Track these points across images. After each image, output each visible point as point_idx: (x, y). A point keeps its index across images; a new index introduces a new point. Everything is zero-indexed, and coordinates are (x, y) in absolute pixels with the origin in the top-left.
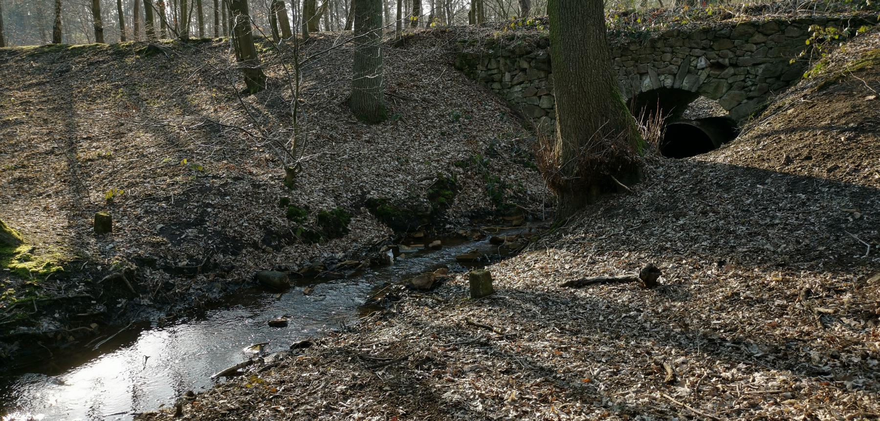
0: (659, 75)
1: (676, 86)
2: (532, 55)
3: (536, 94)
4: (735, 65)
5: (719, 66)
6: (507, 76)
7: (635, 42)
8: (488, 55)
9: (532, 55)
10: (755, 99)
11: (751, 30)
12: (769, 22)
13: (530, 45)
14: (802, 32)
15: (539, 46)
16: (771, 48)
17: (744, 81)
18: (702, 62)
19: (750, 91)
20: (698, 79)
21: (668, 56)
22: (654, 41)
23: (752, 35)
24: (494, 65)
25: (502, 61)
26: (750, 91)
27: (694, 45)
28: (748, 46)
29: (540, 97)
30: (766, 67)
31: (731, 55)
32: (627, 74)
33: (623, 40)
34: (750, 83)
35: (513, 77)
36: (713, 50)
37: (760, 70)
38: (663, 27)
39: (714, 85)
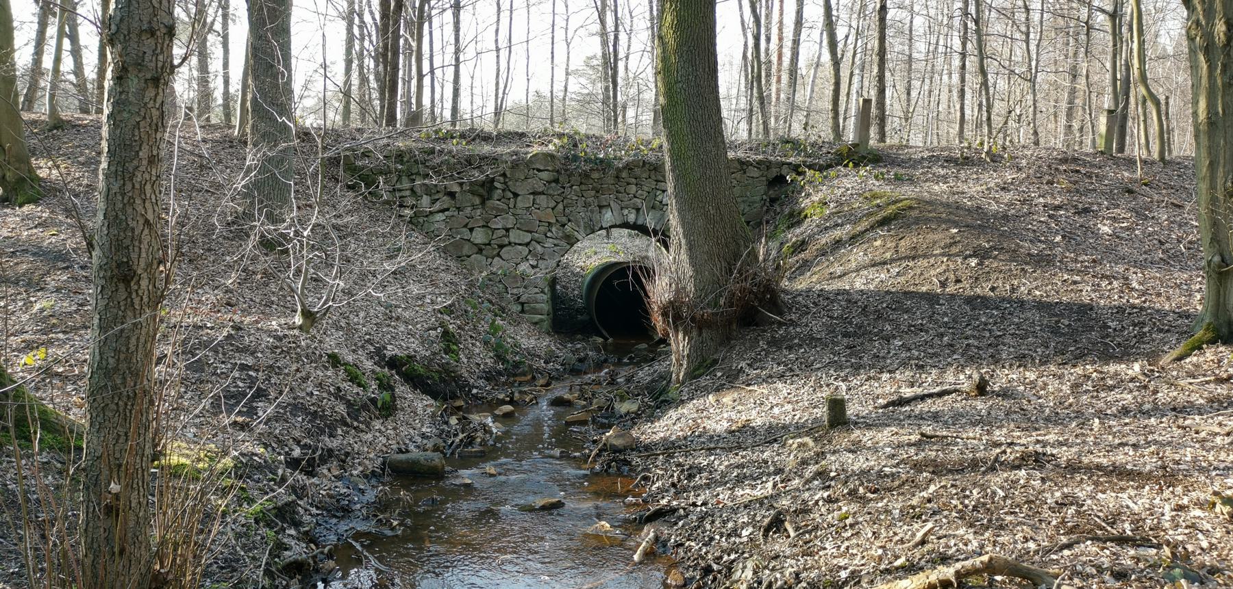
3: (466, 226)
21: (633, 189)
22: (619, 170)
29: (471, 230)
32: (586, 205)
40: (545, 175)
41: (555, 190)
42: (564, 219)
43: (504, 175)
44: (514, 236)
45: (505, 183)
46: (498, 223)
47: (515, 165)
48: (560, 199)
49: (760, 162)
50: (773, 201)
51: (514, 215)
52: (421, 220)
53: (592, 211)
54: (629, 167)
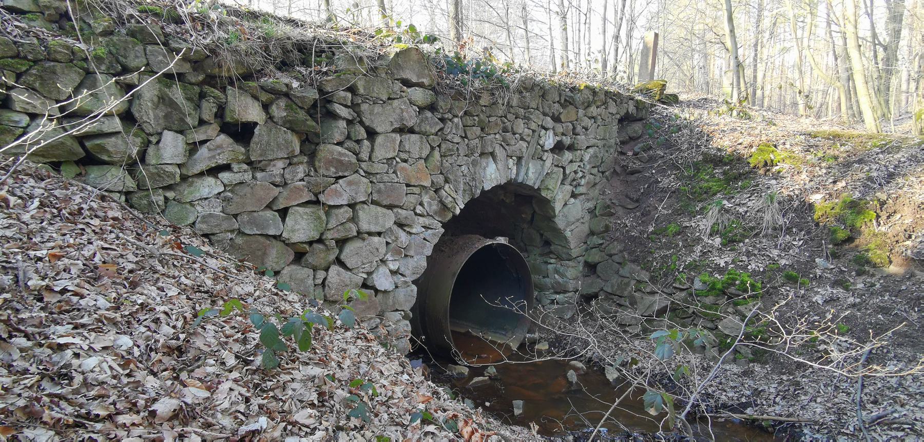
18: (549, 141)
20: (543, 166)
29: (283, 213)
35: (193, 148)
41: (431, 123)
43: (352, 90)
44: (369, 218)
45: (354, 106)
46: (340, 194)
48: (436, 140)
51: (368, 174)
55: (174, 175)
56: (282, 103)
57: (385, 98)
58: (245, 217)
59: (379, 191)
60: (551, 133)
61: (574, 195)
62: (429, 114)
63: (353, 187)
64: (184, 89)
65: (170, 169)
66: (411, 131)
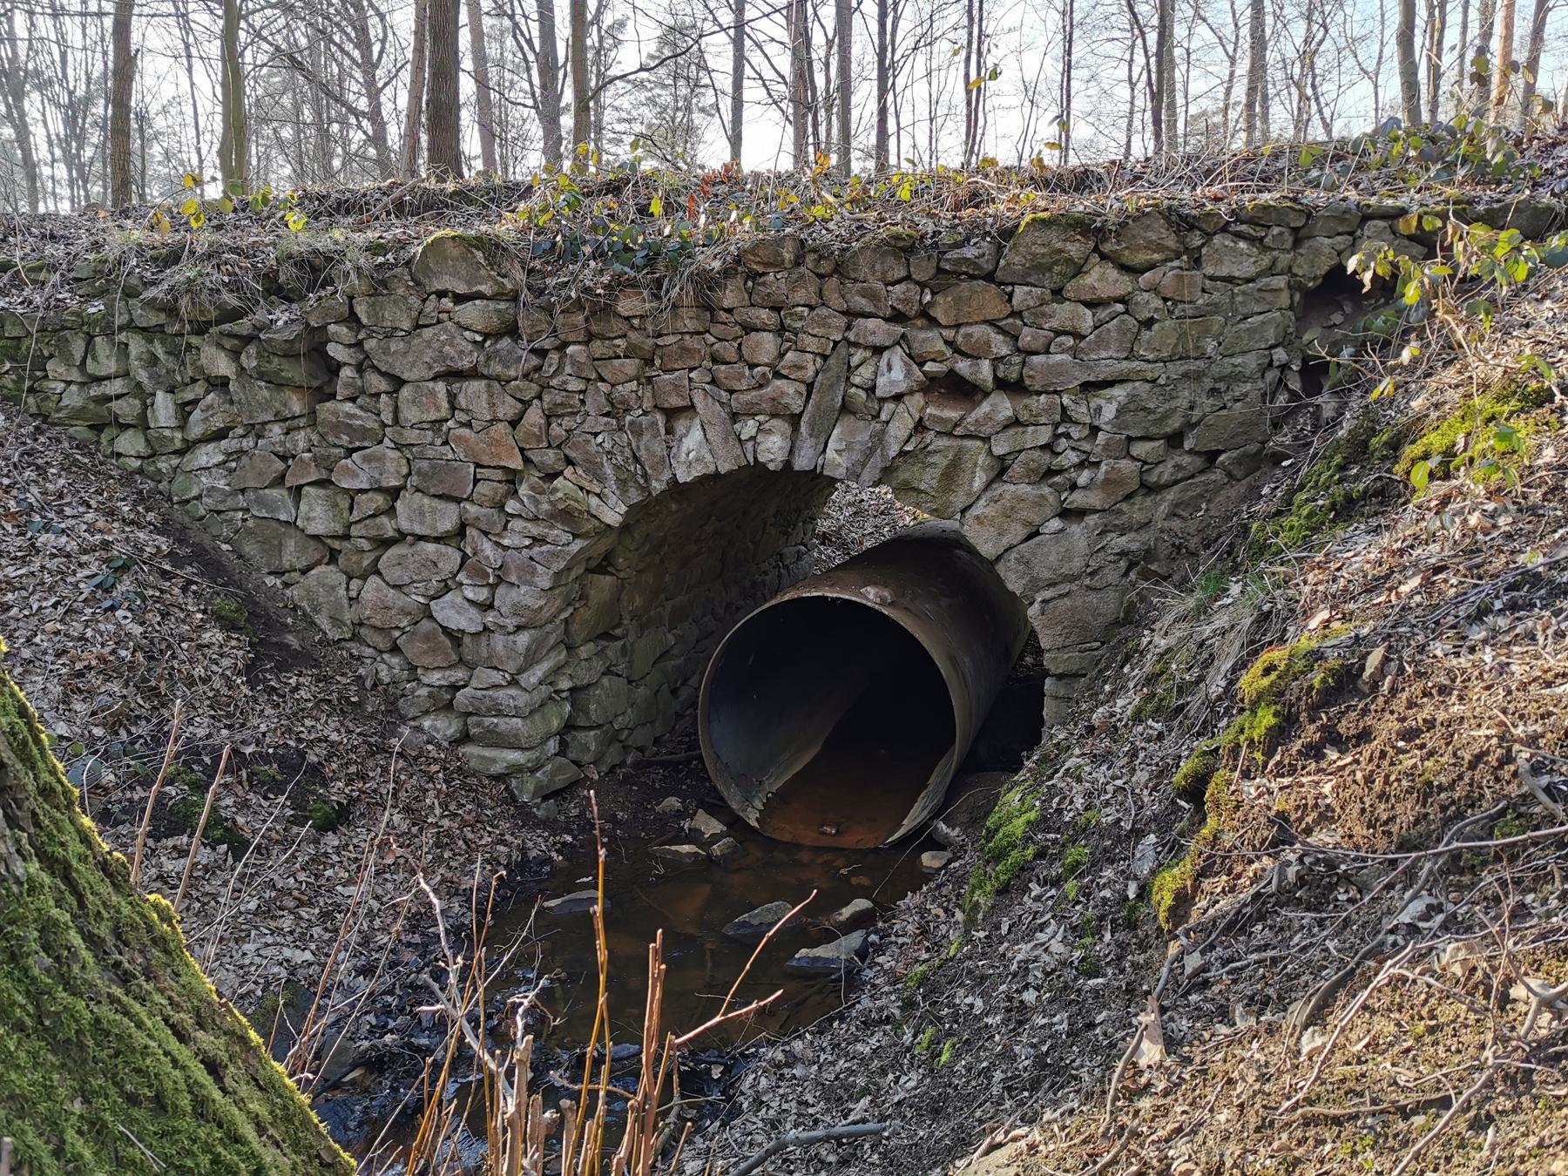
0: (734, 417)
1: (802, 463)
2: (244, 326)
3: (280, 480)
4: (1014, 387)
5: (960, 390)
6: (163, 409)
7: (634, 284)
8: (92, 322)
9: (244, 326)
10: (1092, 520)
11: (1075, 249)
12: (1141, 215)
13: (235, 286)
14: (1266, 261)
15: (276, 290)
16: (1149, 323)
17: (1048, 447)
18: (895, 374)
19: (1074, 487)
20: (879, 438)
21: (766, 345)
22: (706, 283)
23: (1079, 270)
24: (106, 362)
25: (136, 346)
26: (1074, 487)
27: (862, 303)
28: (1062, 314)
29: (297, 492)
30: (1133, 398)
31: (1001, 346)
33: (591, 274)
34: (1073, 457)
35: (184, 410)
36: (933, 322)
37: (1109, 406)
38: (742, 229)
39: (941, 461)
40: (471, 313)
42: (551, 457)
43: (352, 319)
44: (411, 513)
46: (355, 474)
47: (379, 284)
49: (1262, 218)
50: (1314, 373)
51: (398, 447)
52: (163, 465)
53: (638, 431)
54: (746, 267)
55: (172, 440)
56: (252, 349)
57: (406, 325)
58: (251, 495)
59: (419, 473)
60: (897, 357)
61: (1066, 514)
62: (506, 342)
63: (373, 464)
64: (163, 343)
65: (167, 433)
66: (473, 374)
